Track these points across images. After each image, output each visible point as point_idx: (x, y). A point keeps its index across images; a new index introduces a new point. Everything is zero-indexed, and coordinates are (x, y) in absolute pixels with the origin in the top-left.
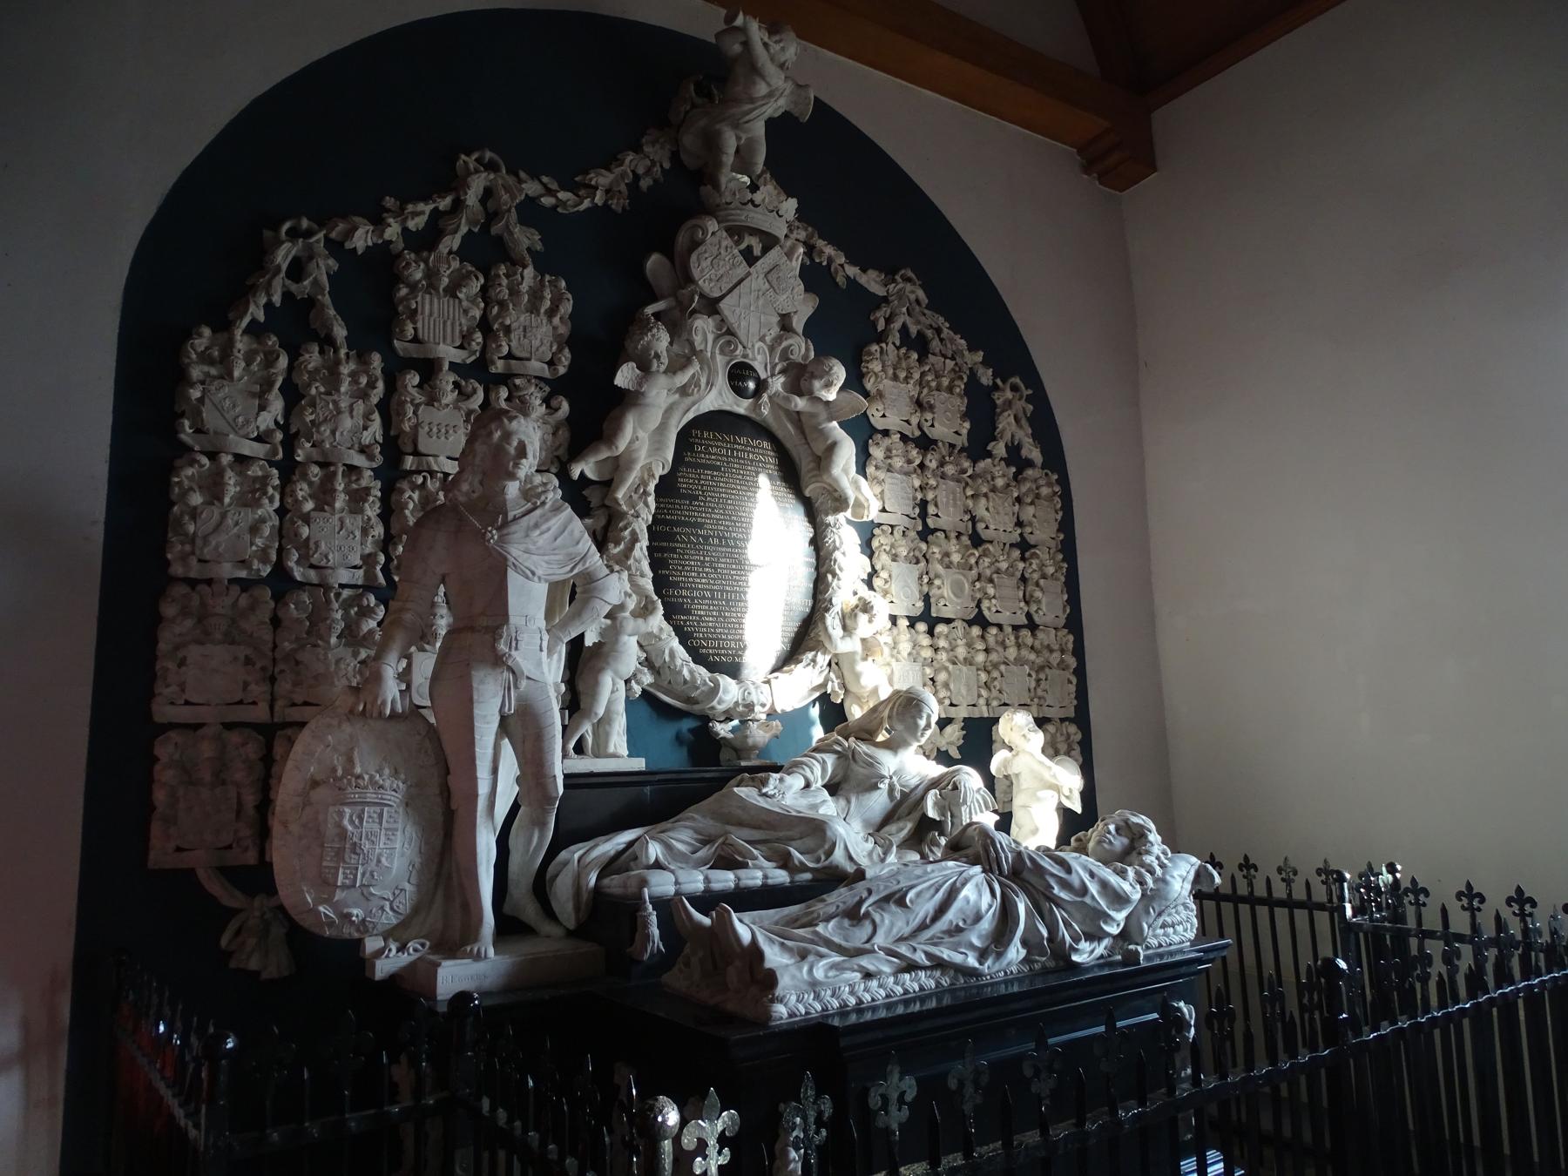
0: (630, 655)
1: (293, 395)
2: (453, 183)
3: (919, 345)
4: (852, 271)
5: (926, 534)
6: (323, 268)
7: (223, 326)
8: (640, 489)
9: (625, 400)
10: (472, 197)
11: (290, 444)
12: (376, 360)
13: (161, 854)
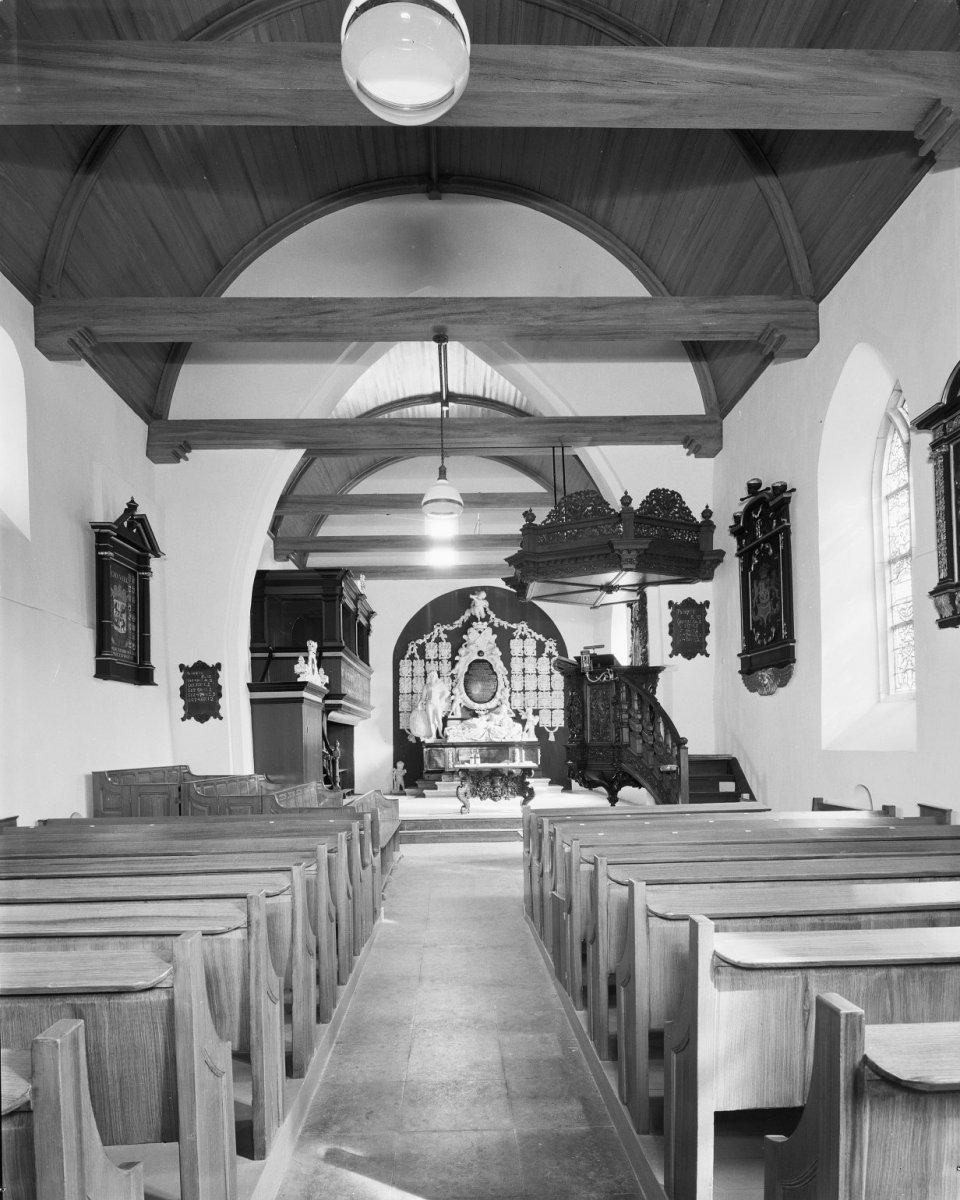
1: (413, 667)
2: (433, 629)
3: (523, 637)
4: (510, 625)
5: (524, 675)
6: (416, 648)
10: (436, 631)
13: (401, 728)
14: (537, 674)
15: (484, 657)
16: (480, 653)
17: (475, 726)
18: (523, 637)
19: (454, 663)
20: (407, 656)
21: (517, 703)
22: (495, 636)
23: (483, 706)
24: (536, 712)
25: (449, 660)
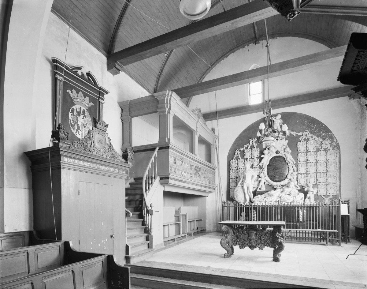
0: (263, 181)
2: (249, 142)
4: (297, 134)
5: (307, 163)
6: (239, 153)
7: (233, 159)
8: (265, 166)
9: (263, 158)
11: (237, 168)
12: (243, 159)
13: (231, 197)
14: (317, 162)
15: (280, 155)
16: (277, 152)
17: (272, 195)
18: (307, 140)
19: (261, 159)
20: (235, 158)
21: (302, 181)
22: (287, 141)
23: (279, 184)
24: (316, 186)
25: (258, 158)
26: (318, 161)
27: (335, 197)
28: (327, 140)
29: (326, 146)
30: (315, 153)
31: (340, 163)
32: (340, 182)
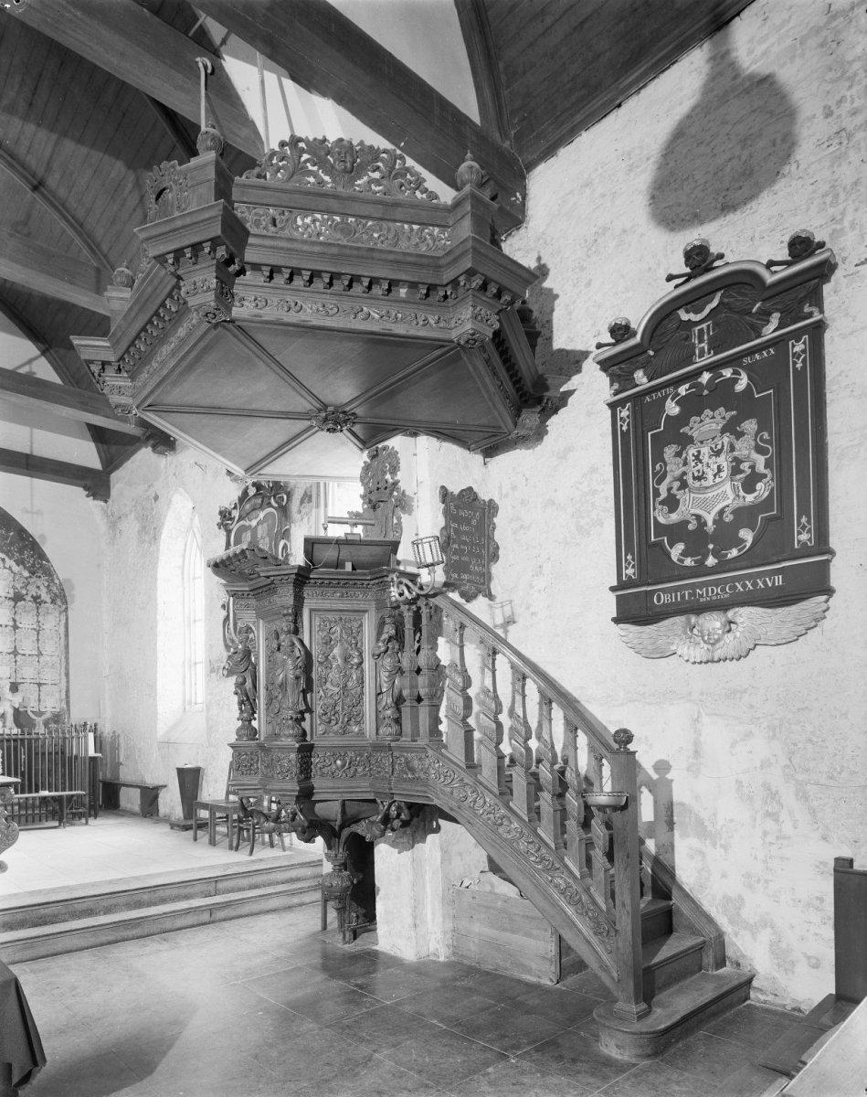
14: (15, 627)
26: (20, 625)
27: (57, 718)
28: (40, 577)
29: (36, 590)
30: (12, 603)
31: (67, 635)
32: (68, 682)
